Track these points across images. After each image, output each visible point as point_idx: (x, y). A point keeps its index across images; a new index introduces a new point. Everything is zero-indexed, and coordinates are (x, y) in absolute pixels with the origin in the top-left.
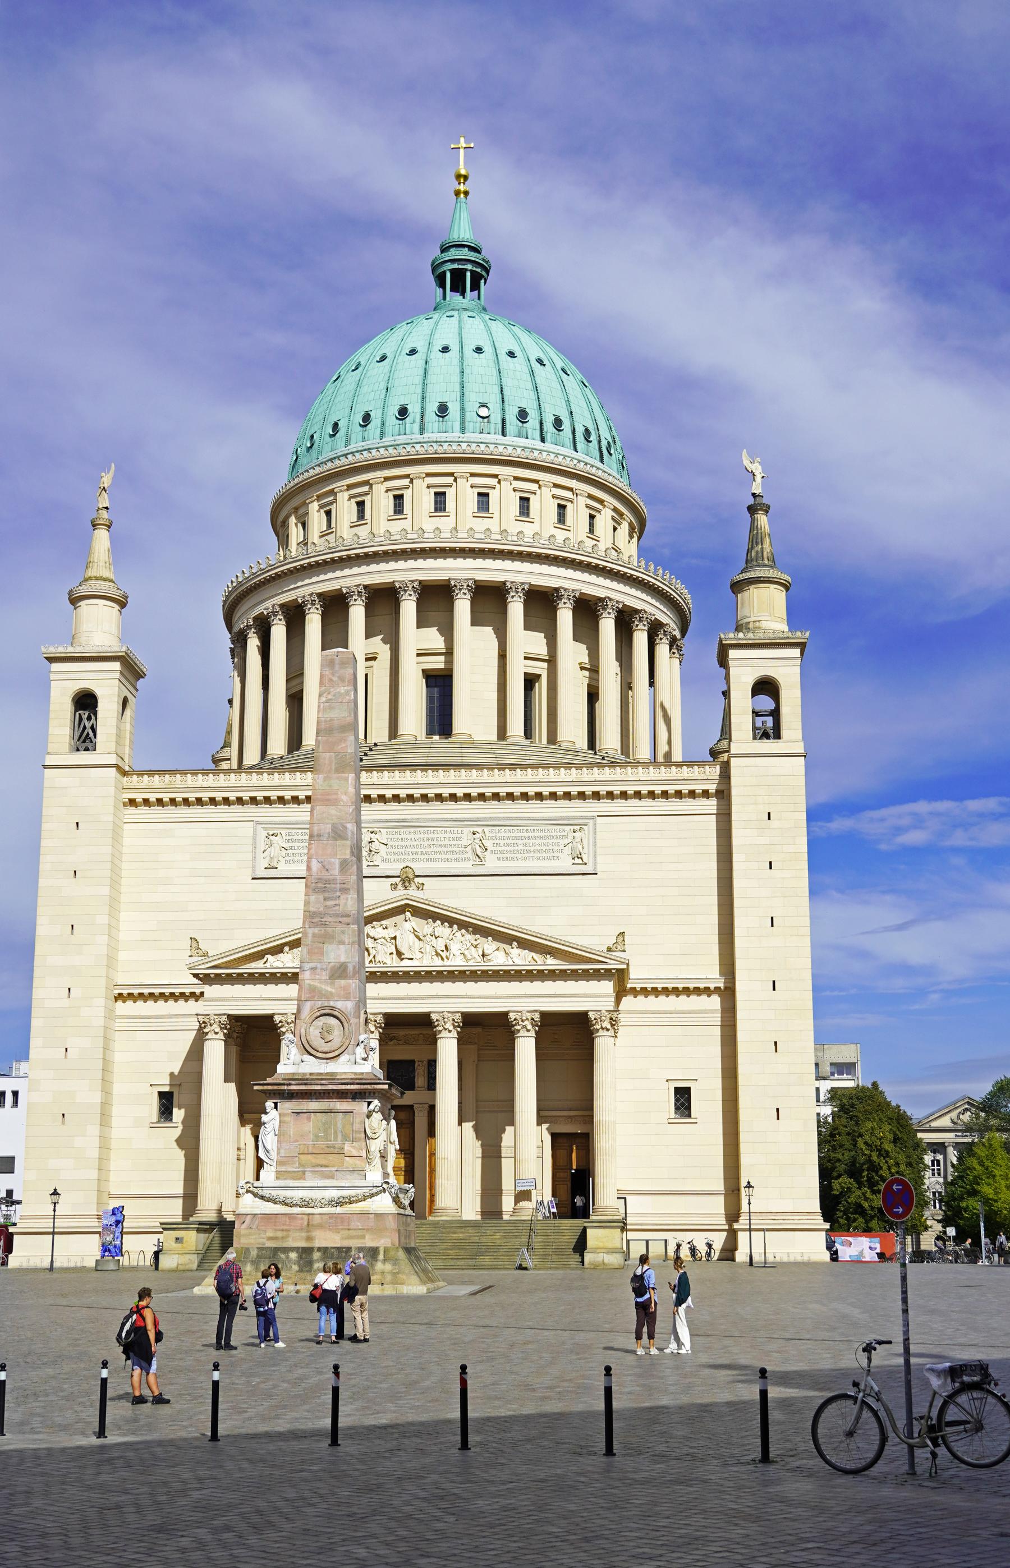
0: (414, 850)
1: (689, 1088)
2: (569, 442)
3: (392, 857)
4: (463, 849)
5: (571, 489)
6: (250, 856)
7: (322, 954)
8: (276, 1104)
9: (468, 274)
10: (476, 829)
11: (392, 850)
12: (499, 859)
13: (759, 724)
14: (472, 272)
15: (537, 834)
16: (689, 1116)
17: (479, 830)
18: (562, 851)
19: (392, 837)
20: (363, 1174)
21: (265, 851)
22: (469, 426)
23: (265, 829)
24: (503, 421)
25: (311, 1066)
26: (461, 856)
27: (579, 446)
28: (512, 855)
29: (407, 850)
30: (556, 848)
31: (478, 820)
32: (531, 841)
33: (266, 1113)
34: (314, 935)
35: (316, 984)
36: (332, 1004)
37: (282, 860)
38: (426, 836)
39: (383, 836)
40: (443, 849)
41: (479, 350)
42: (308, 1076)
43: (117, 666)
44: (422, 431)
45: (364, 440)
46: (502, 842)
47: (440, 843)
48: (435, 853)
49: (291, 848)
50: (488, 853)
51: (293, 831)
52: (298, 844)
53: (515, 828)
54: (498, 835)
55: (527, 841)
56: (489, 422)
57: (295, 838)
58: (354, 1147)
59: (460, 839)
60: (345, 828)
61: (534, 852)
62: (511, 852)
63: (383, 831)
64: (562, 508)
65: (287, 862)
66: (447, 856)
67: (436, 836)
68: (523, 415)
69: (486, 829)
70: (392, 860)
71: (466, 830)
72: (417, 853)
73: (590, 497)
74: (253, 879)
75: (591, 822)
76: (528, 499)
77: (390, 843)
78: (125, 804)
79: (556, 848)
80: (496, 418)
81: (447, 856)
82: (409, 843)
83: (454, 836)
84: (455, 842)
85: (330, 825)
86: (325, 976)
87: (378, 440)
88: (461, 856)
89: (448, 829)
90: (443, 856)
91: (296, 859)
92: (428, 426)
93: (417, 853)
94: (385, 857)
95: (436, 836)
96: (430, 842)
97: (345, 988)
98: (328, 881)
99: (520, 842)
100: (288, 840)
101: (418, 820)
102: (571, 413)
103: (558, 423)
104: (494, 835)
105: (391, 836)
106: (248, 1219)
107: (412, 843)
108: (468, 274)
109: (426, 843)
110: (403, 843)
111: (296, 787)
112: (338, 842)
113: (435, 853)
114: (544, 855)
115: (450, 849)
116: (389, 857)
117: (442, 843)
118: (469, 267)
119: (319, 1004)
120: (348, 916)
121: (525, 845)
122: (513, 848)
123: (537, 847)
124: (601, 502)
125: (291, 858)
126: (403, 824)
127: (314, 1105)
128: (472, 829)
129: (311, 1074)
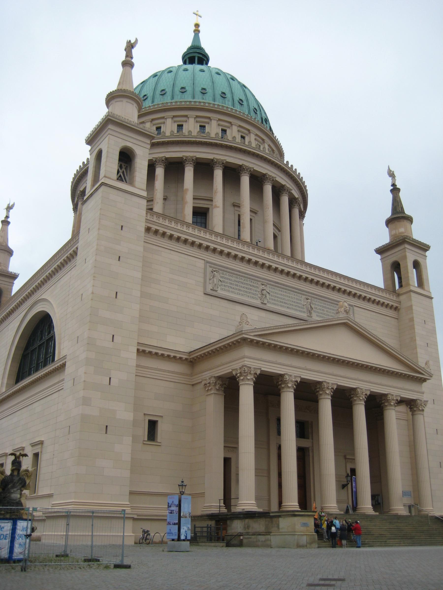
0: (282, 300)
3: (272, 301)
4: (302, 306)
6: (202, 280)
11: (272, 298)
15: (331, 307)
17: (310, 298)
19: (272, 290)
21: (210, 279)
23: (210, 267)
26: (302, 310)
28: (323, 315)
29: (279, 299)
31: (308, 292)
37: (219, 287)
38: (286, 294)
39: (268, 289)
40: (294, 304)
46: (318, 307)
47: (293, 300)
48: (291, 305)
49: (224, 282)
51: (225, 273)
52: (228, 281)
53: (323, 302)
54: (316, 303)
55: (327, 310)
57: (225, 276)
59: (301, 300)
63: (268, 286)
65: (222, 289)
66: (296, 308)
67: (291, 296)
69: (312, 299)
70: (272, 303)
72: (283, 302)
74: (205, 294)
77: (271, 293)
81: (296, 308)
82: (279, 296)
83: (297, 297)
84: (298, 301)
88: (302, 310)
89: (296, 294)
90: (294, 307)
91: (226, 288)
93: (283, 302)
94: (269, 300)
95: (291, 296)
96: (288, 298)
99: (325, 310)
100: (222, 277)
101: (284, 285)
104: (315, 303)
105: (271, 290)
107: (281, 296)
110: (277, 295)
113: (291, 305)
115: (297, 305)
116: (270, 301)
117: (294, 300)
121: (327, 311)
122: (322, 312)
125: (223, 287)
126: (276, 284)
128: (307, 297)
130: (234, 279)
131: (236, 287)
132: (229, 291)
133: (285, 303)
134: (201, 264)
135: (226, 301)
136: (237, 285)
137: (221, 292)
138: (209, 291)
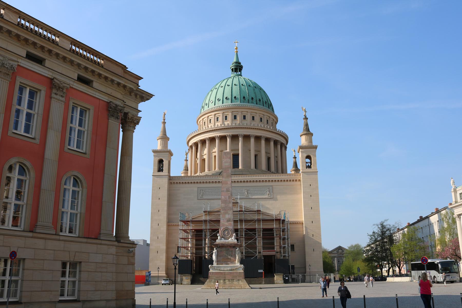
1: (294, 245)
2: (262, 104)
5: (263, 114)
7: (225, 216)
8: (216, 249)
9: (238, 69)
10: (246, 189)
12: (251, 195)
13: (307, 165)
14: (239, 68)
15: (260, 190)
16: (294, 251)
18: (265, 193)
20: (235, 264)
21: (200, 194)
22: (241, 101)
23: (200, 189)
24: (248, 100)
25: (223, 241)
27: (264, 105)
30: (264, 193)
32: (258, 191)
33: (214, 250)
34: (223, 212)
35: (224, 223)
36: (227, 227)
38: (235, 190)
41: (242, 85)
42: (223, 243)
43: (168, 153)
44: (231, 103)
45: (218, 104)
49: (206, 193)
50: (249, 194)
56: (245, 100)
58: (233, 258)
60: (229, 189)
61: (260, 193)
62: (254, 193)
64: (261, 119)
68: (252, 99)
69: (249, 188)
71: (244, 189)
73: (267, 115)
75: (271, 187)
76: (254, 117)
78: (169, 183)
79: (264, 193)
80: (247, 100)
85: (226, 189)
86: (226, 221)
87: (222, 104)
89: (240, 189)
92: (232, 101)
97: (230, 224)
98: (226, 201)
99: (256, 191)
102: (262, 98)
103: (260, 100)
106: (211, 273)
108: (238, 69)
109: (235, 192)
111: (207, 180)
112: (228, 192)
114: (261, 194)
117: (239, 192)
118: (239, 67)
119: (225, 227)
120: (230, 208)
122: (254, 193)
123: (260, 193)
124: (269, 117)
127: (224, 249)
129: (224, 242)
130: (210, 190)
131: (211, 194)
132: (208, 196)
133: (234, 194)
134: (196, 189)
135: (207, 200)
136: (211, 193)
137: (204, 197)
138: (199, 198)
